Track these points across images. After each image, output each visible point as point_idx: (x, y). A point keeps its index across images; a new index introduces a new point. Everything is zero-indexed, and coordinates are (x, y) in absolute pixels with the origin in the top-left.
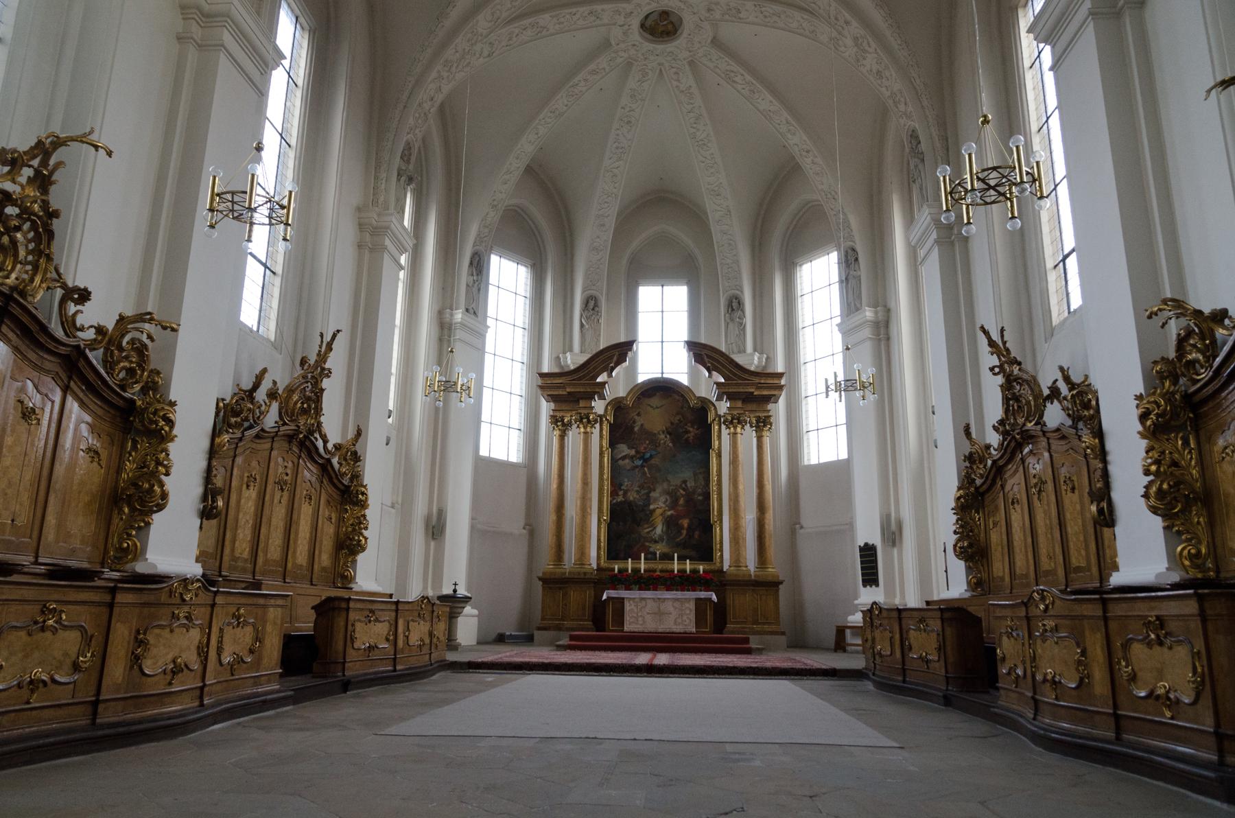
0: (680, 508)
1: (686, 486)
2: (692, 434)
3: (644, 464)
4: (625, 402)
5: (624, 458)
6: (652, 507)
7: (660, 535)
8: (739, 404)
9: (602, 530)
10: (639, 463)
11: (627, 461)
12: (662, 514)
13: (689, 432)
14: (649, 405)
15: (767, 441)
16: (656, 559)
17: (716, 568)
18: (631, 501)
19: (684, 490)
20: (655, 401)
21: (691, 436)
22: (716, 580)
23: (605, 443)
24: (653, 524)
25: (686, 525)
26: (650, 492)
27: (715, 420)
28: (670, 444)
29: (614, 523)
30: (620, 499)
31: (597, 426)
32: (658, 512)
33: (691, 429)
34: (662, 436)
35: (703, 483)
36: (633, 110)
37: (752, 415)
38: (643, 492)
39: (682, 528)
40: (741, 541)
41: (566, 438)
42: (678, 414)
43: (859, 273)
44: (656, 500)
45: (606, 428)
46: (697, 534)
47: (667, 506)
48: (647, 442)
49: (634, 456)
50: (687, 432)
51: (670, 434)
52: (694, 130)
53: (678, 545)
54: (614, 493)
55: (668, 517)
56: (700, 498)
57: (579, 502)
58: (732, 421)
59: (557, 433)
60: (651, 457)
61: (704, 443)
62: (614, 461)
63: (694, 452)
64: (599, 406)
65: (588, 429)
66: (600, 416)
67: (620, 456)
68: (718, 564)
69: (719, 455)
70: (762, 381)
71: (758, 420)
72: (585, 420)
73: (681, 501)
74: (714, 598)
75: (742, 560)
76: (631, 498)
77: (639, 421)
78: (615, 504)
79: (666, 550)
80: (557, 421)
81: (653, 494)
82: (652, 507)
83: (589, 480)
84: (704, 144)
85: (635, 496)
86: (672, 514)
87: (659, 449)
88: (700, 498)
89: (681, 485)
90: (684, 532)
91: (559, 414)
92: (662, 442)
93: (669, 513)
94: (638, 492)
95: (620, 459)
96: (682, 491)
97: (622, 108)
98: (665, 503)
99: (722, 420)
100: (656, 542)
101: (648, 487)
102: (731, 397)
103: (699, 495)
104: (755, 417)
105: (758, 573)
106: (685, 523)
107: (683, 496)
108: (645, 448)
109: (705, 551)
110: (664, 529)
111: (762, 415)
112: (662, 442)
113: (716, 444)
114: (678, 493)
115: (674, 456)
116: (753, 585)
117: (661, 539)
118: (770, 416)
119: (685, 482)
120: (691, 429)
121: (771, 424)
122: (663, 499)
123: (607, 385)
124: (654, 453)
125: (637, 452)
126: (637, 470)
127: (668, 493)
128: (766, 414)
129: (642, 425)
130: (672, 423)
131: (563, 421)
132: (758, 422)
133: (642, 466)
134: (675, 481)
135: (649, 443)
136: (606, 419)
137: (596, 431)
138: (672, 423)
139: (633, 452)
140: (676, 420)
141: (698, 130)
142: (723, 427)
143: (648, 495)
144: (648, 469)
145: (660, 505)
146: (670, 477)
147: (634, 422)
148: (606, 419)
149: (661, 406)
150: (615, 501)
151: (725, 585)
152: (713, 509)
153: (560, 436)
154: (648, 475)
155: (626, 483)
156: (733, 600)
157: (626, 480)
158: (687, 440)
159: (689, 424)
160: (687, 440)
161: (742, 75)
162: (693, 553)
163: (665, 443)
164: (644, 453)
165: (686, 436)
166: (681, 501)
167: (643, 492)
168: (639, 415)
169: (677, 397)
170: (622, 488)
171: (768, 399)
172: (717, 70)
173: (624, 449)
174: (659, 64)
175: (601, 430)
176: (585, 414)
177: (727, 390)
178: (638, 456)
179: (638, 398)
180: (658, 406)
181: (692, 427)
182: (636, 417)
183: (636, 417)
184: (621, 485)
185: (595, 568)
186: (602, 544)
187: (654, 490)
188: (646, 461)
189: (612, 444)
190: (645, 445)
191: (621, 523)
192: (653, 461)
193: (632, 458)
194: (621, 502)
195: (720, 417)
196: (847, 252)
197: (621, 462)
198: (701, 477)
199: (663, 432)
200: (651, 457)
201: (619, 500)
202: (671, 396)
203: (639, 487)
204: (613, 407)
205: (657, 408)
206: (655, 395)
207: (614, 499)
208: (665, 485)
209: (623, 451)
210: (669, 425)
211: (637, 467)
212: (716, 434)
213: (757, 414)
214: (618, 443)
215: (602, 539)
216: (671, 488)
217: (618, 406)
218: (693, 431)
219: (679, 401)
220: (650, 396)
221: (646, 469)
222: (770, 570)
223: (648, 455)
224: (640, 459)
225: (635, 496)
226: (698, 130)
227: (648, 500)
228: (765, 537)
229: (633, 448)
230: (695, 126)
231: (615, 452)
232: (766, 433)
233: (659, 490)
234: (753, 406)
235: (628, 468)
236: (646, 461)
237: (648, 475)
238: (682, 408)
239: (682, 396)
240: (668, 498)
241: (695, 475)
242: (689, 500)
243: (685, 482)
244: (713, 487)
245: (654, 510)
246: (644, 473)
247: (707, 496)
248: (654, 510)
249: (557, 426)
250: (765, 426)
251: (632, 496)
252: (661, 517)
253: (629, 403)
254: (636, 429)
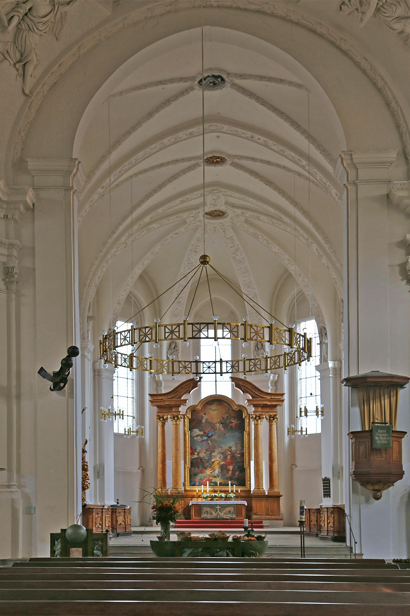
0: (228, 461)
1: (231, 449)
2: (234, 424)
3: (208, 439)
4: (197, 408)
5: (197, 436)
6: (213, 460)
7: (217, 474)
8: (260, 409)
9: (187, 472)
10: (205, 438)
11: (199, 437)
12: (218, 464)
13: (232, 422)
14: (210, 409)
15: (274, 427)
16: (217, 486)
17: (247, 490)
18: (202, 457)
19: (230, 451)
20: (214, 407)
21: (233, 425)
22: (247, 496)
23: (187, 428)
24: (214, 469)
25: (231, 469)
26: (212, 453)
27: (246, 416)
28: (222, 429)
29: (193, 468)
30: (195, 456)
31: (182, 420)
32: (216, 462)
33: (233, 421)
34: (218, 425)
35: (240, 448)
36: (198, 246)
37: (267, 414)
38: (208, 453)
39: (229, 470)
40: (260, 477)
41: (165, 426)
42: (226, 413)
43: (326, 341)
44: (215, 457)
45: (187, 421)
46: (237, 473)
47: (221, 460)
48: (210, 428)
49: (203, 435)
50: (231, 422)
51: (222, 424)
52: (235, 255)
53: (227, 478)
54: (192, 454)
55: (222, 465)
56: (239, 455)
57: (174, 458)
58: (256, 418)
59: (160, 424)
60: (212, 435)
61: (241, 427)
62: (192, 437)
63: (235, 433)
64: (183, 409)
65: (178, 422)
66: (184, 415)
67: (195, 435)
68: (248, 488)
69: (249, 435)
70: (272, 398)
71: (270, 417)
72: (176, 418)
73: (229, 457)
74: (246, 504)
75: (260, 486)
76: (202, 456)
77: (205, 417)
78: (193, 459)
79: (222, 481)
80: (160, 418)
81: (213, 454)
82: (213, 460)
83: (179, 448)
84: (241, 262)
85: (204, 455)
86: (224, 464)
87: (216, 431)
88: (239, 455)
89: (228, 450)
90: (231, 472)
91: (161, 415)
92: (218, 428)
93: (222, 463)
94: (205, 453)
95: (195, 436)
96: (229, 452)
97: (193, 245)
98: (220, 458)
99: (251, 416)
100: (215, 477)
101: (211, 450)
102: (255, 406)
103: (238, 454)
104: (268, 415)
105: (269, 492)
106: (231, 468)
107: (229, 454)
108: (209, 431)
109: (242, 481)
110: (220, 471)
111: (272, 414)
112: (218, 428)
113: (247, 428)
114: (227, 453)
115: (225, 435)
116: (266, 498)
117: (218, 476)
118: (276, 415)
119: (230, 448)
120: (233, 421)
121: (277, 419)
122: (219, 456)
123: (187, 401)
124: (213, 433)
125: (204, 433)
126: (204, 442)
127: (222, 453)
128: (275, 414)
129: (207, 419)
130: (223, 418)
131: (163, 418)
132: (270, 417)
133: (207, 440)
134: (225, 447)
135: (210, 429)
136: (187, 417)
137: (181, 423)
138: (223, 418)
139: (202, 433)
140: (225, 416)
141: (237, 255)
142: (251, 420)
143: (210, 455)
144: (211, 441)
145: (217, 458)
146: (222, 445)
147: (202, 418)
148: (187, 417)
149: (217, 409)
150: (193, 458)
151: (252, 497)
152: (246, 461)
153: (162, 425)
154: (210, 444)
155: (199, 448)
156: (256, 504)
157: (198, 447)
158: (231, 426)
159: (232, 419)
160: (231, 426)
161: (262, 236)
162: (235, 482)
163: (219, 428)
164: (208, 434)
165: (230, 425)
166: (229, 457)
167: (208, 453)
168: (205, 414)
169: (226, 405)
170: (197, 451)
171: (275, 406)
172: (248, 232)
173: (197, 431)
174: (214, 227)
175: (184, 422)
176: (176, 415)
177: (252, 403)
178: (205, 435)
179: (204, 405)
180: (216, 409)
181: (234, 420)
182: (203, 415)
183: (203, 415)
184: (196, 449)
185: (183, 490)
186: (187, 479)
187: (214, 452)
188: (209, 437)
189: (191, 429)
190: (208, 430)
191: (197, 468)
192: (213, 437)
193: (201, 436)
194: (196, 458)
195: (249, 415)
196: (321, 328)
197: (195, 438)
198: (239, 445)
199: (218, 423)
200: (212, 435)
201: (195, 457)
202: (222, 404)
203: (206, 450)
204: (190, 410)
205: (215, 410)
206: (214, 403)
207: (192, 456)
208: (220, 449)
209: (196, 433)
210: (222, 419)
211: (204, 440)
212: (247, 424)
213: (270, 414)
214: (193, 429)
215: (187, 476)
216: (223, 450)
217: (193, 410)
218: (235, 422)
219: (227, 406)
220: (211, 404)
221: (209, 441)
222: (275, 490)
223: (210, 435)
224: (206, 436)
225: (204, 455)
226: (237, 255)
227: (211, 457)
228: (273, 474)
229: (202, 431)
230: (235, 253)
231: (192, 433)
232: (274, 424)
233: (217, 451)
234: (268, 410)
235: (200, 441)
236: (209, 437)
237: (210, 444)
238: (229, 410)
239: (229, 404)
240: (221, 455)
241: (236, 444)
242: (233, 457)
243: (230, 448)
244: (246, 451)
245: (214, 462)
246: (209, 443)
247: (242, 455)
248: (214, 462)
249: (160, 420)
250: (274, 420)
251: (202, 455)
252: (218, 465)
253: (199, 408)
254: (203, 421)
